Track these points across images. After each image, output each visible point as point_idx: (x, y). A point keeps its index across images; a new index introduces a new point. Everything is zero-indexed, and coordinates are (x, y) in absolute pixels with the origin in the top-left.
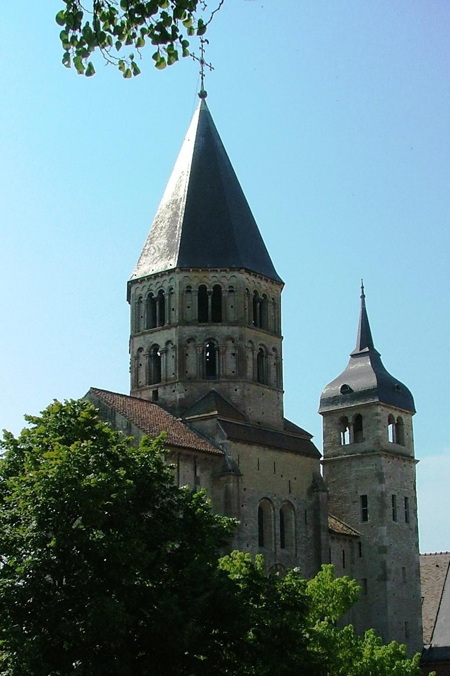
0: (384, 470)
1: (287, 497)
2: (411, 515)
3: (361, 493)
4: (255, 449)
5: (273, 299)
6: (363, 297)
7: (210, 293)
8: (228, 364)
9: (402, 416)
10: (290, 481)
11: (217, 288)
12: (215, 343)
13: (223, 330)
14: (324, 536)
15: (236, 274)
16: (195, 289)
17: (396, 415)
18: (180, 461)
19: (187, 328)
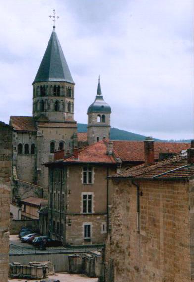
0: (94, 131)
6: (99, 80)
8: (46, 107)
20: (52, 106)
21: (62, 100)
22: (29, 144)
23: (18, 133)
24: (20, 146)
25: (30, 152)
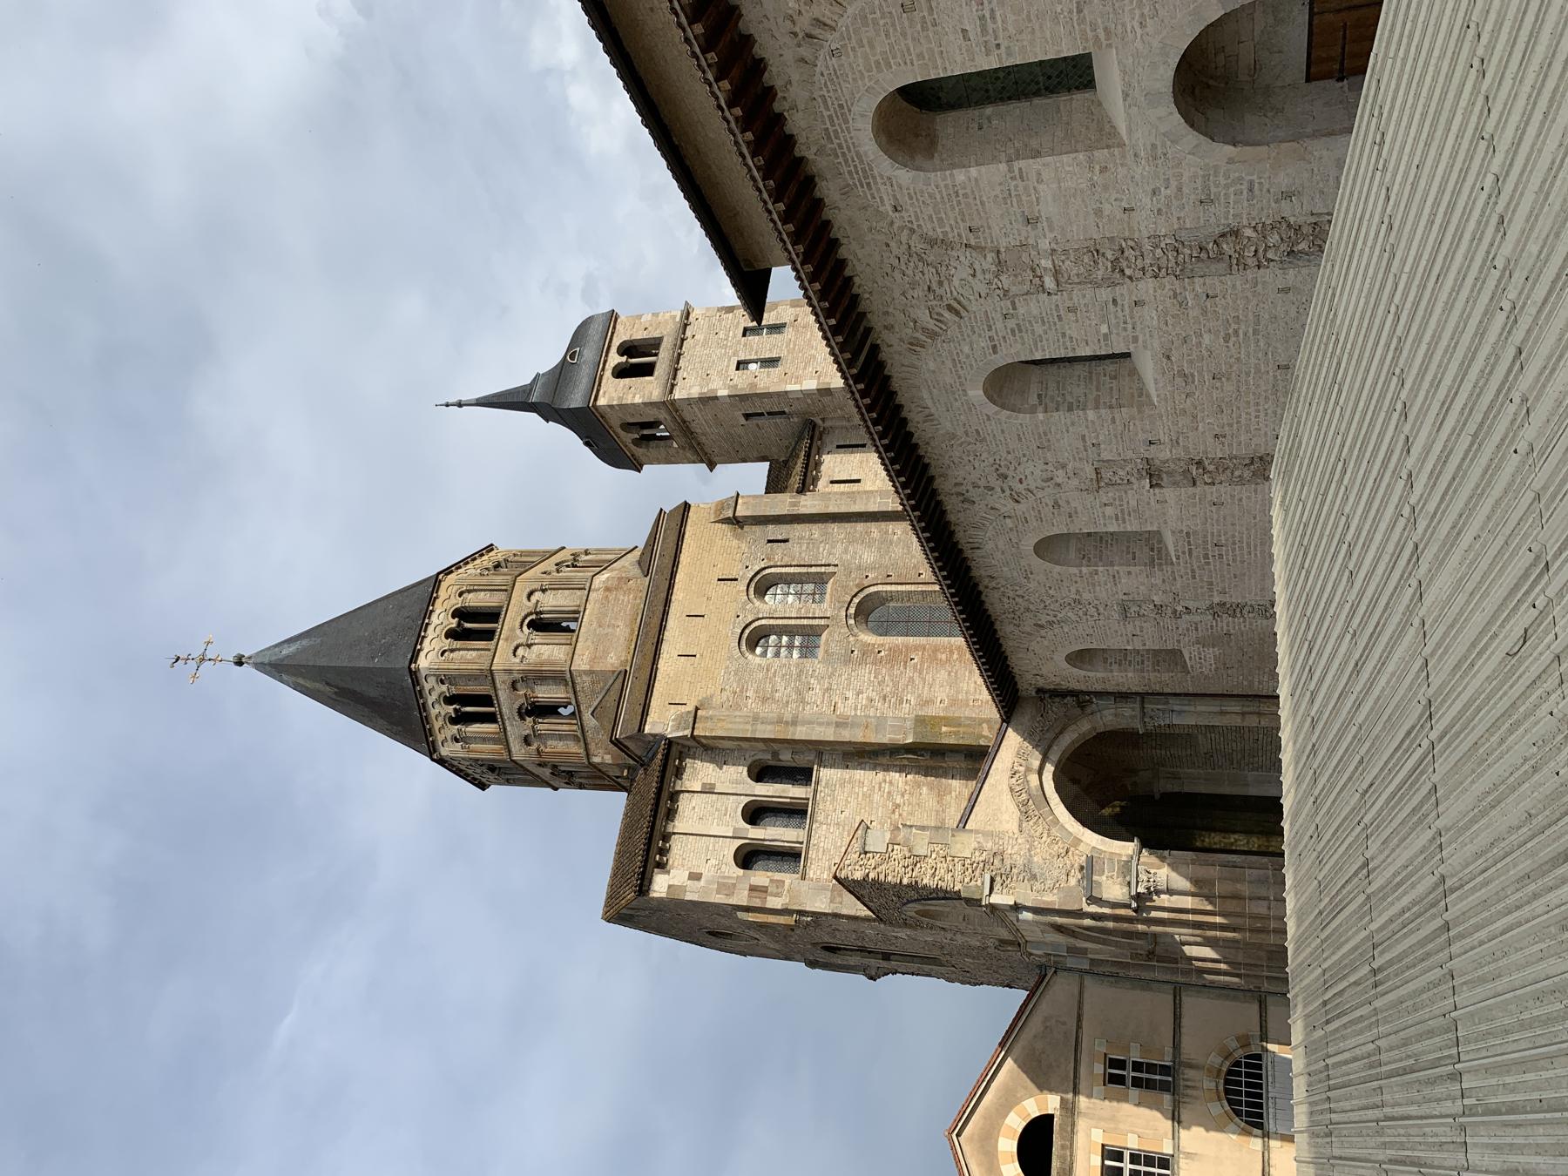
0: (695, 392)
3: (743, 421)
4: (662, 664)
6: (460, 405)
9: (616, 343)
11: (449, 700)
13: (503, 694)
14: (808, 504)
17: (615, 359)
20: (547, 651)
23: (662, 866)
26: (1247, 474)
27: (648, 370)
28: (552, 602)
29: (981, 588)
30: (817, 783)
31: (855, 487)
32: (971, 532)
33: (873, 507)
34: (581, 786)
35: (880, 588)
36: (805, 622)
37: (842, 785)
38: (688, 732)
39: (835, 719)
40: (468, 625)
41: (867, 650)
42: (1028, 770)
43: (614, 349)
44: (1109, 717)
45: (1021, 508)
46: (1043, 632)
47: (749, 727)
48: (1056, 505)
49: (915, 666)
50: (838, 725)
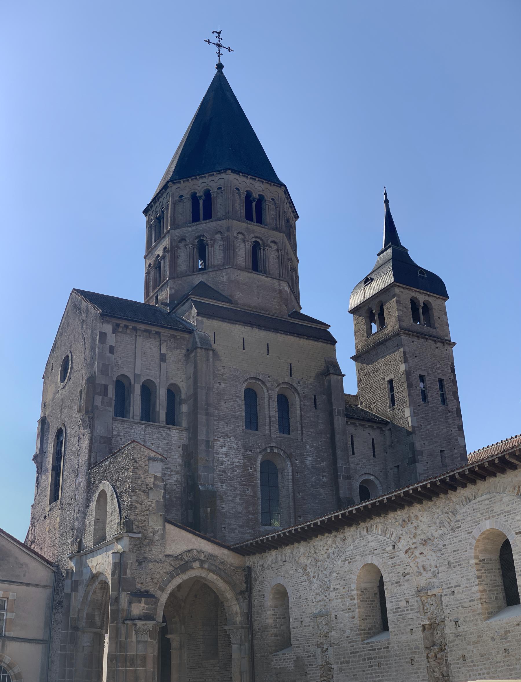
1: (287, 380)
2: (449, 397)
3: (387, 379)
5: (273, 199)
6: (387, 201)
7: (200, 197)
8: (216, 254)
9: (431, 300)
10: (290, 364)
12: (204, 239)
14: (339, 421)
15: (223, 175)
16: (187, 195)
17: (422, 298)
18: (137, 337)
19: (177, 231)
20: (242, 254)
21: (274, 242)
22: (157, 381)
24: (122, 387)
25: (162, 415)
26: (437, 675)
27: (416, 318)
28: (271, 257)
29: (334, 533)
30: (169, 429)
31: (350, 452)
32: (380, 527)
33: (340, 463)
34: (148, 273)
35: (290, 468)
36: (267, 421)
37: (168, 444)
38: (199, 344)
39: (211, 439)
40: (254, 204)
41: (251, 460)
42: (202, 562)
43: (427, 298)
44: (235, 608)
45: (402, 555)
46: (300, 570)
47: (204, 385)
48: (405, 575)
49: (244, 491)
50: (207, 442)
